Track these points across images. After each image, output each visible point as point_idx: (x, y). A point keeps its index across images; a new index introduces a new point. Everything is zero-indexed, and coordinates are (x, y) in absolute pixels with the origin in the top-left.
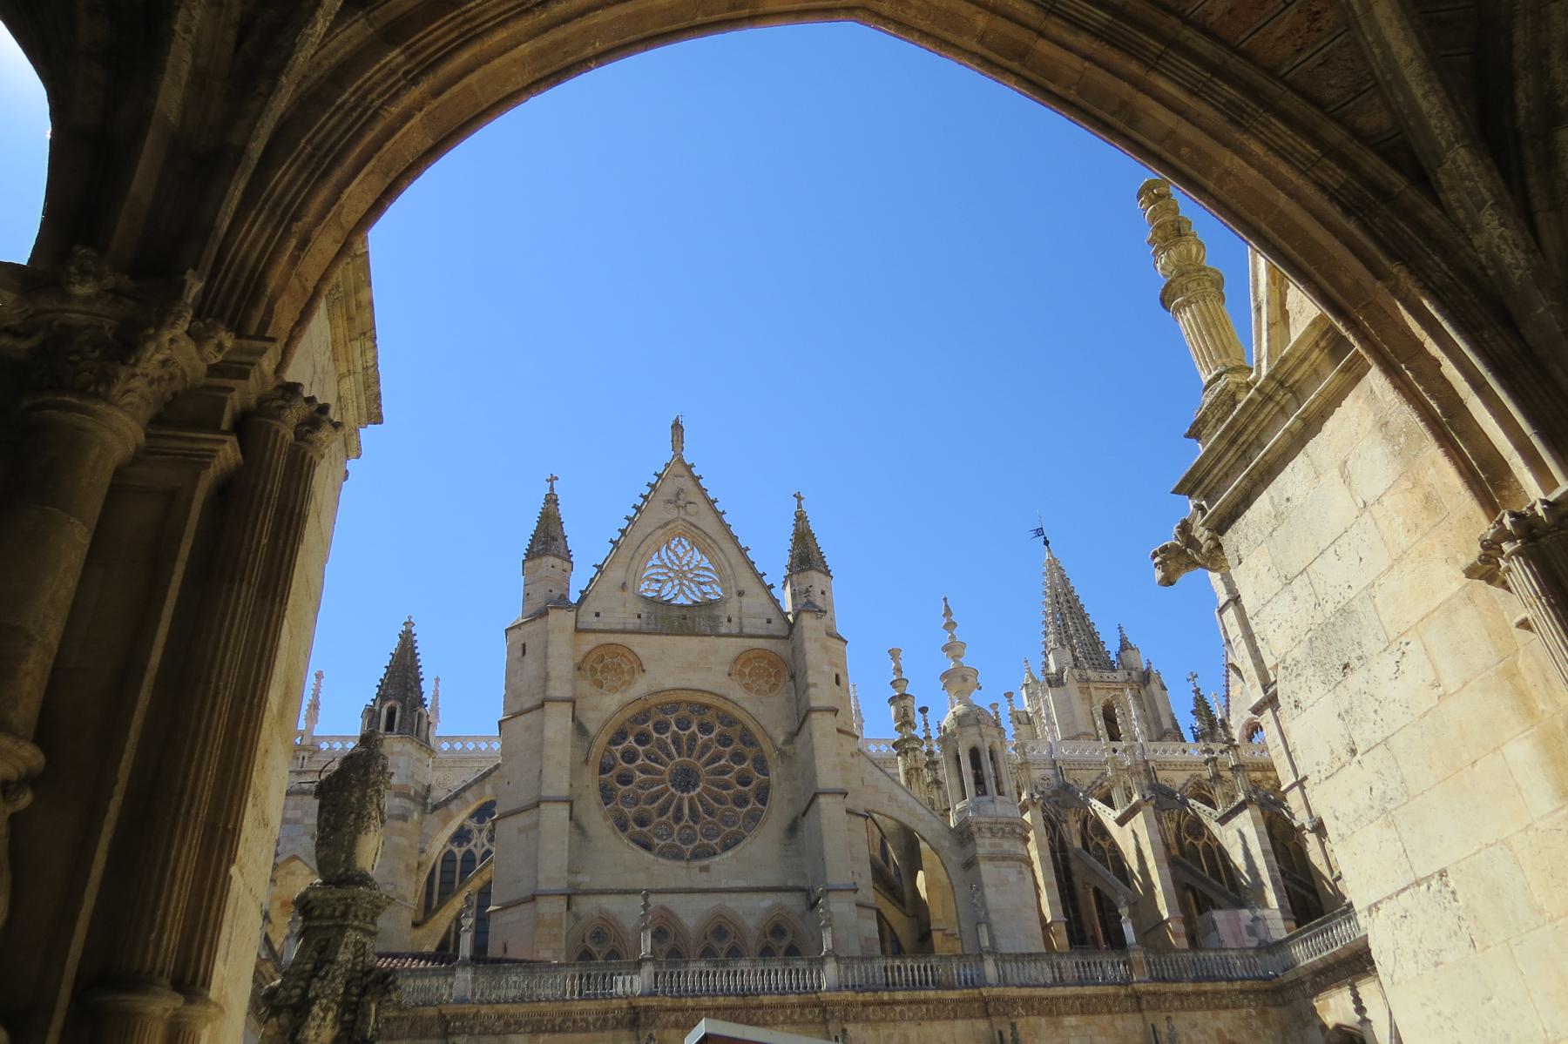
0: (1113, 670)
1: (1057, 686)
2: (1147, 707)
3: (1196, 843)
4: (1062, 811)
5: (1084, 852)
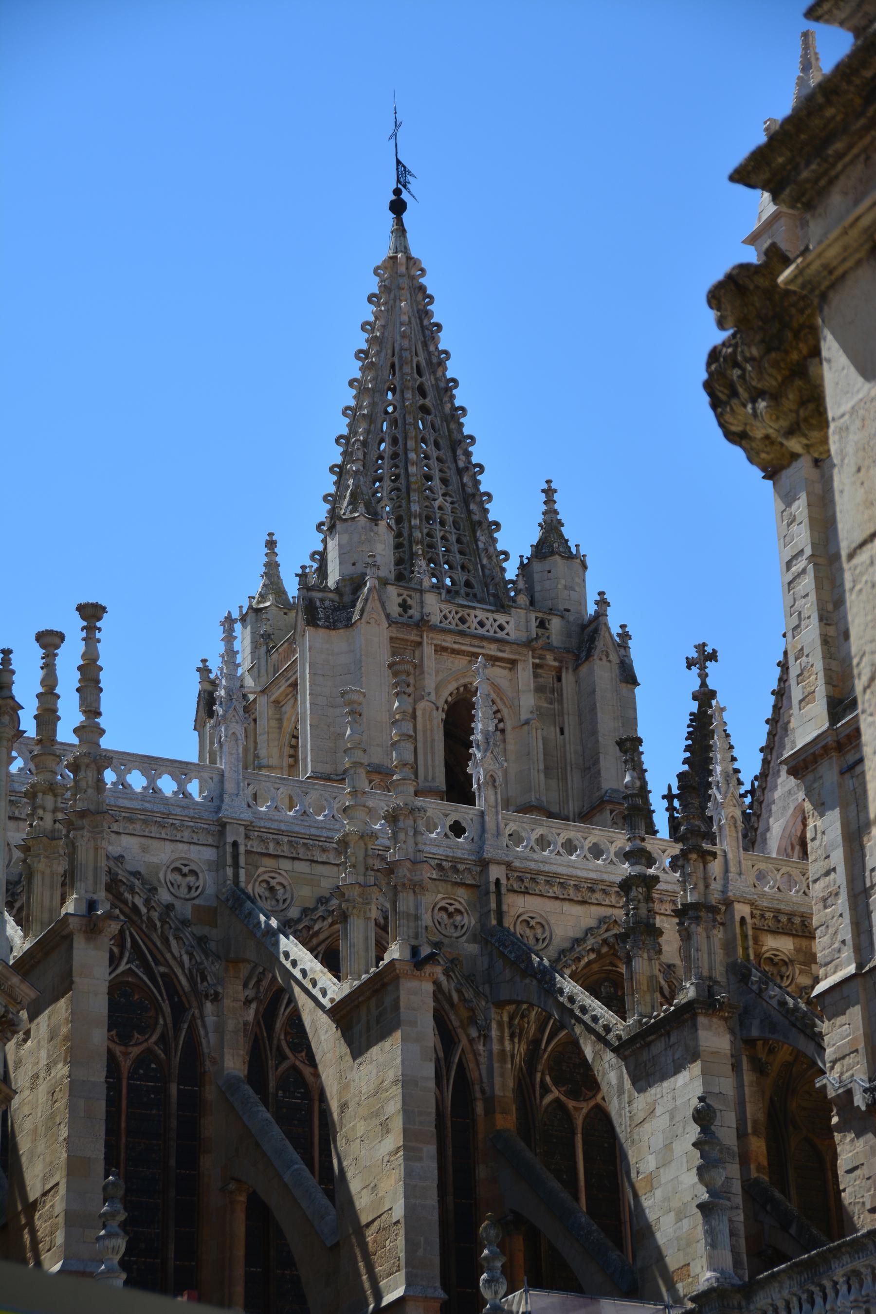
0: (502, 605)
1: (332, 626)
2: (570, 723)
3: (571, 1104)
4: (214, 968)
5: (248, 1089)
